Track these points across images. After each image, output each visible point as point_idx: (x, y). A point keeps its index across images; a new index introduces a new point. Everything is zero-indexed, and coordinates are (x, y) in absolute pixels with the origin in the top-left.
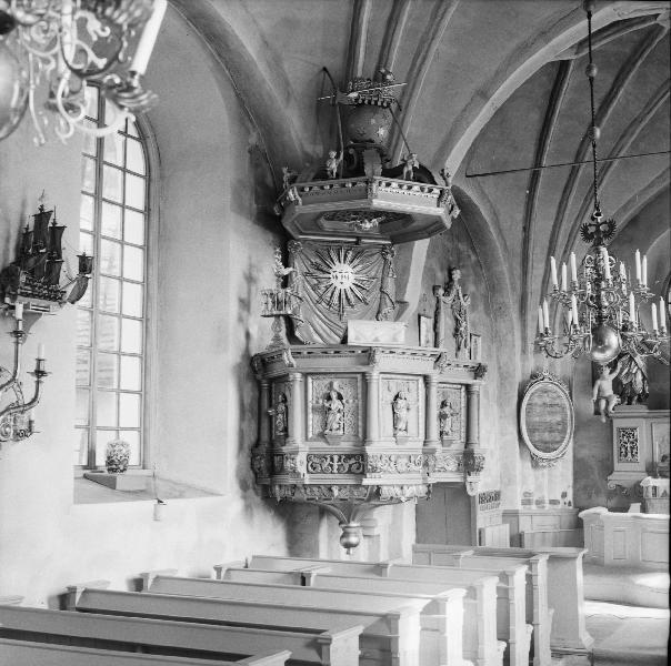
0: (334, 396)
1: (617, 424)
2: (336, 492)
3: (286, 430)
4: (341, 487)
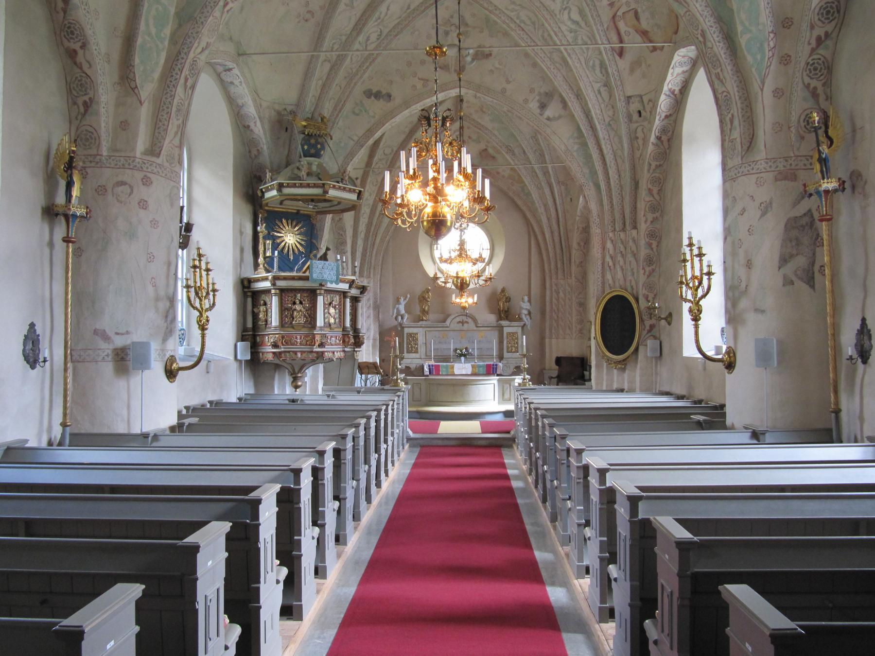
0: (298, 302)
1: (406, 330)
2: (299, 355)
3: (266, 321)
4: (302, 352)
